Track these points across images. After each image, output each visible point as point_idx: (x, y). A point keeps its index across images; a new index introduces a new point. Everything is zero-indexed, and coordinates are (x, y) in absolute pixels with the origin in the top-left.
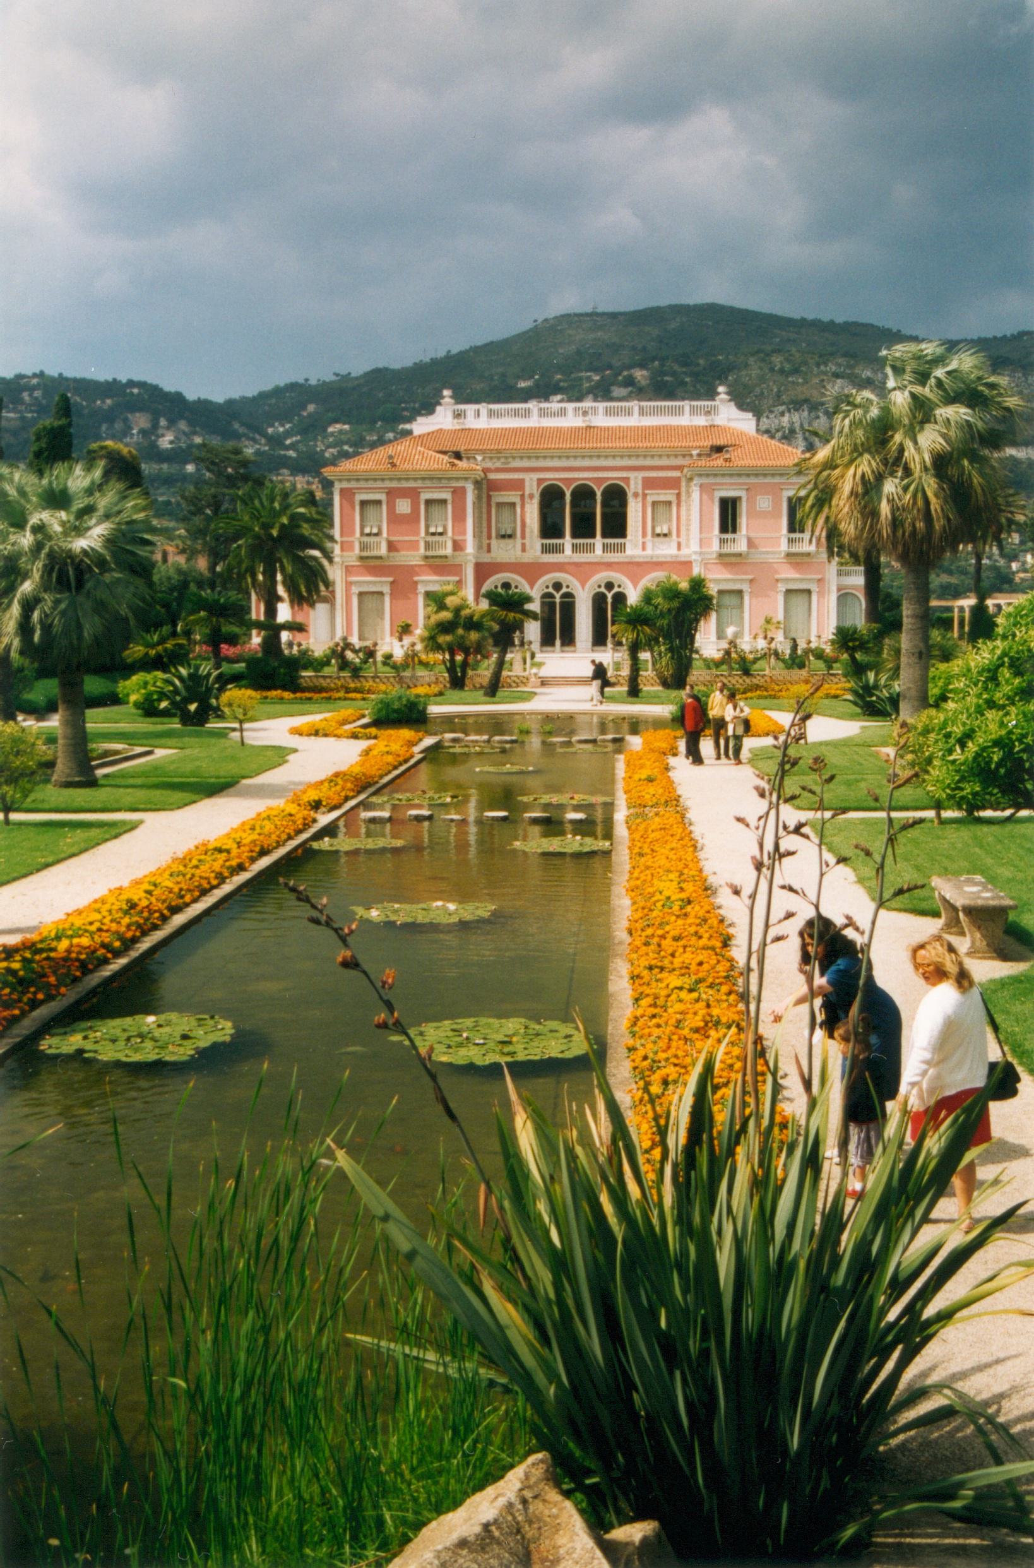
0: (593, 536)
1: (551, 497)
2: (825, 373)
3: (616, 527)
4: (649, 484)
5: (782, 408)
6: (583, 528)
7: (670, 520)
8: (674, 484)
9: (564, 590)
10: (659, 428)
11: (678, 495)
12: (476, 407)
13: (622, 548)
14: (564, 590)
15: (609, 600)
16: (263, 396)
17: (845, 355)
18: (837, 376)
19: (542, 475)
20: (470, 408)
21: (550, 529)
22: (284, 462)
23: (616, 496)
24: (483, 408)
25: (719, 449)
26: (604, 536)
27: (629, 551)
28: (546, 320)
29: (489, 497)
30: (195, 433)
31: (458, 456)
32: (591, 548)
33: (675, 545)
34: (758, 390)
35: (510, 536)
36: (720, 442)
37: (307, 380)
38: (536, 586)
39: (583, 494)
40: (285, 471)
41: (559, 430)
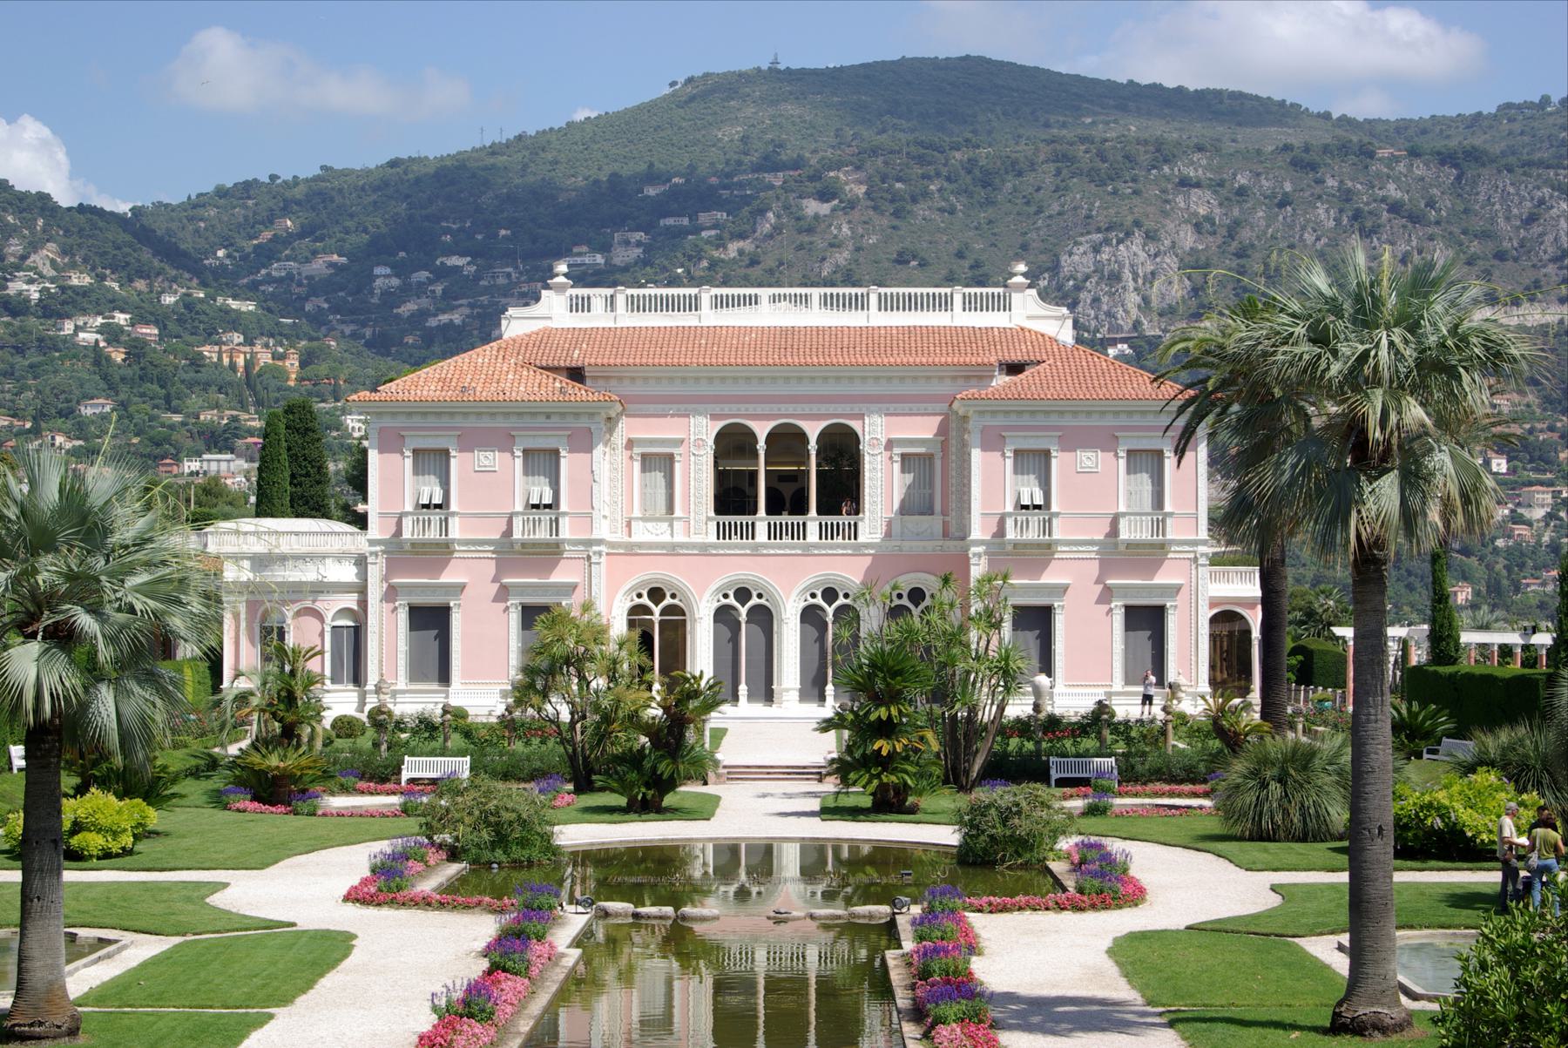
1: (733, 443)
2: (1168, 180)
3: (842, 491)
5: (1098, 237)
6: (786, 500)
9: (754, 601)
10: (910, 330)
12: (609, 291)
14: (754, 601)
16: (196, 204)
17: (1200, 149)
18: (1185, 183)
19: (717, 409)
20: (598, 295)
21: (732, 497)
22: (234, 321)
24: (622, 295)
25: (1014, 369)
26: (821, 511)
28: (690, 80)
30: (73, 266)
31: (576, 374)
34: (1055, 208)
36: (1015, 357)
37: (273, 177)
40: (238, 338)
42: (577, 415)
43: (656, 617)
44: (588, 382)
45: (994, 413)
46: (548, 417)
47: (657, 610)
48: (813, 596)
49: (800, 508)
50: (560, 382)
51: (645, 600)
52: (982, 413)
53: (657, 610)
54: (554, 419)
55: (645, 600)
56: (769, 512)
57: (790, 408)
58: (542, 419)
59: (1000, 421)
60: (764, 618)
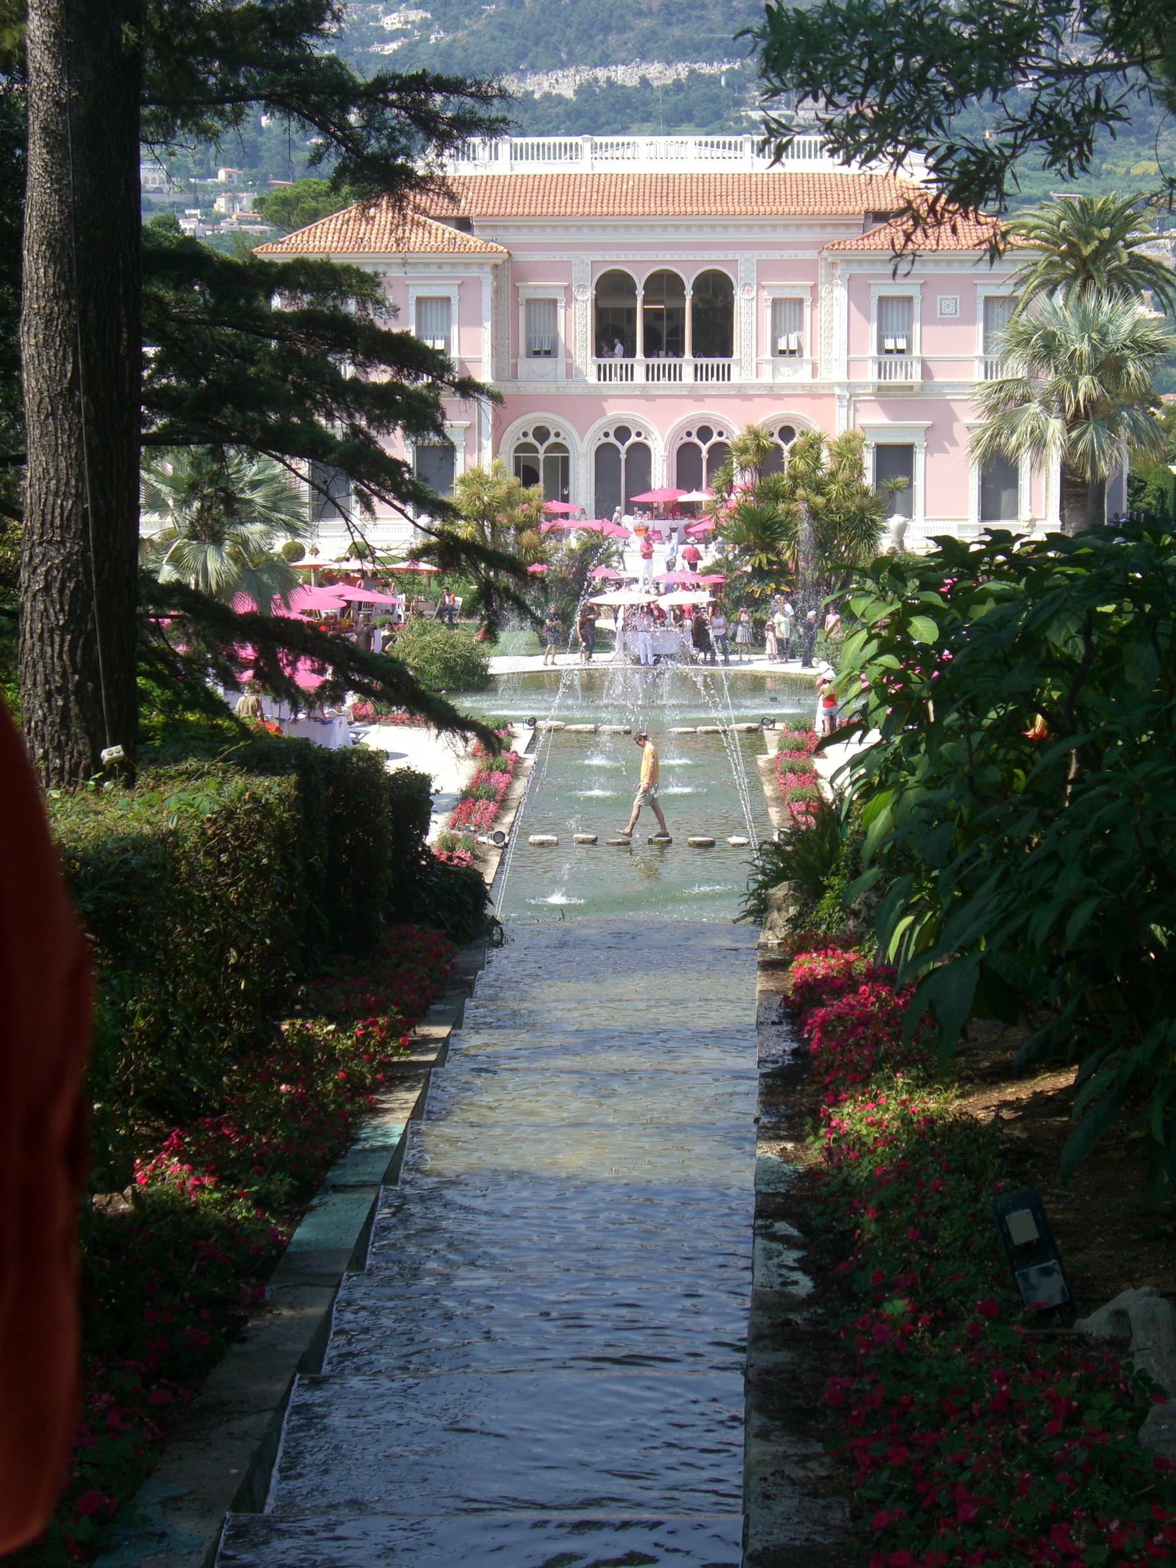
0: (678, 352)
1: (613, 287)
3: (715, 338)
4: (765, 269)
6: (663, 340)
7: (801, 328)
8: (809, 269)
11: (814, 288)
13: (726, 373)
15: (705, 455)
23: (716, 294)
27: (735, 378)
29: (516, 289)
32: (674, 373)
33: (809, 368)
35: (548, 353)
38: (589, 434)
39: (664, 283)
41: (624, 178)
42: (467, 265)
43: (541, 456)
44: (476, 231)
45: (860, 262)
46: (440, 266)
47: (542, 449)
48: (689, 434)
49: (677, 350)
50: (451, 231)
51: (531, 439)
52: (849, 262)
53: (542, 449)
54: (446, 269)
55: (531, 439)
56: (648, 354)
57: (667, 256)
58: (434, 269)
59: (866, 270)
60: (641, 453)
